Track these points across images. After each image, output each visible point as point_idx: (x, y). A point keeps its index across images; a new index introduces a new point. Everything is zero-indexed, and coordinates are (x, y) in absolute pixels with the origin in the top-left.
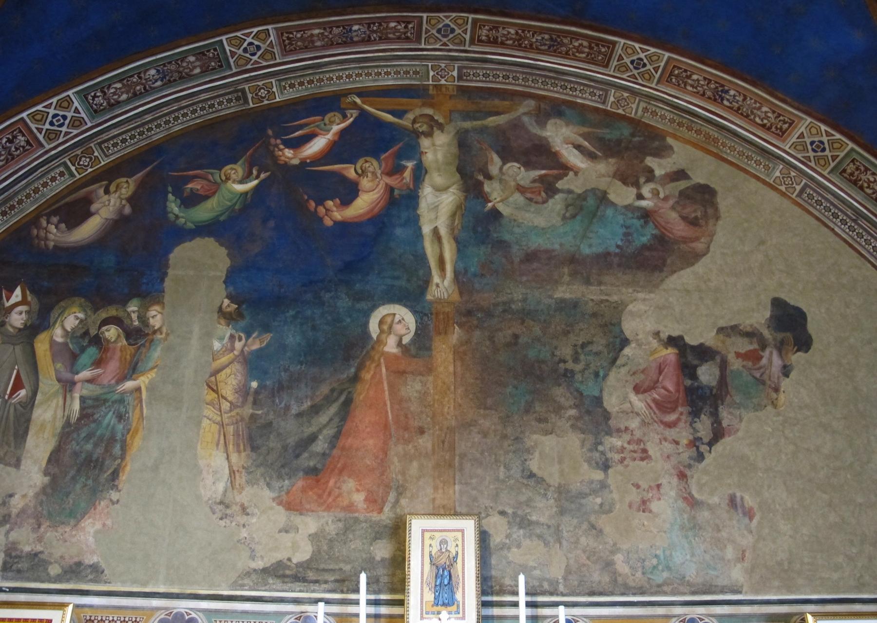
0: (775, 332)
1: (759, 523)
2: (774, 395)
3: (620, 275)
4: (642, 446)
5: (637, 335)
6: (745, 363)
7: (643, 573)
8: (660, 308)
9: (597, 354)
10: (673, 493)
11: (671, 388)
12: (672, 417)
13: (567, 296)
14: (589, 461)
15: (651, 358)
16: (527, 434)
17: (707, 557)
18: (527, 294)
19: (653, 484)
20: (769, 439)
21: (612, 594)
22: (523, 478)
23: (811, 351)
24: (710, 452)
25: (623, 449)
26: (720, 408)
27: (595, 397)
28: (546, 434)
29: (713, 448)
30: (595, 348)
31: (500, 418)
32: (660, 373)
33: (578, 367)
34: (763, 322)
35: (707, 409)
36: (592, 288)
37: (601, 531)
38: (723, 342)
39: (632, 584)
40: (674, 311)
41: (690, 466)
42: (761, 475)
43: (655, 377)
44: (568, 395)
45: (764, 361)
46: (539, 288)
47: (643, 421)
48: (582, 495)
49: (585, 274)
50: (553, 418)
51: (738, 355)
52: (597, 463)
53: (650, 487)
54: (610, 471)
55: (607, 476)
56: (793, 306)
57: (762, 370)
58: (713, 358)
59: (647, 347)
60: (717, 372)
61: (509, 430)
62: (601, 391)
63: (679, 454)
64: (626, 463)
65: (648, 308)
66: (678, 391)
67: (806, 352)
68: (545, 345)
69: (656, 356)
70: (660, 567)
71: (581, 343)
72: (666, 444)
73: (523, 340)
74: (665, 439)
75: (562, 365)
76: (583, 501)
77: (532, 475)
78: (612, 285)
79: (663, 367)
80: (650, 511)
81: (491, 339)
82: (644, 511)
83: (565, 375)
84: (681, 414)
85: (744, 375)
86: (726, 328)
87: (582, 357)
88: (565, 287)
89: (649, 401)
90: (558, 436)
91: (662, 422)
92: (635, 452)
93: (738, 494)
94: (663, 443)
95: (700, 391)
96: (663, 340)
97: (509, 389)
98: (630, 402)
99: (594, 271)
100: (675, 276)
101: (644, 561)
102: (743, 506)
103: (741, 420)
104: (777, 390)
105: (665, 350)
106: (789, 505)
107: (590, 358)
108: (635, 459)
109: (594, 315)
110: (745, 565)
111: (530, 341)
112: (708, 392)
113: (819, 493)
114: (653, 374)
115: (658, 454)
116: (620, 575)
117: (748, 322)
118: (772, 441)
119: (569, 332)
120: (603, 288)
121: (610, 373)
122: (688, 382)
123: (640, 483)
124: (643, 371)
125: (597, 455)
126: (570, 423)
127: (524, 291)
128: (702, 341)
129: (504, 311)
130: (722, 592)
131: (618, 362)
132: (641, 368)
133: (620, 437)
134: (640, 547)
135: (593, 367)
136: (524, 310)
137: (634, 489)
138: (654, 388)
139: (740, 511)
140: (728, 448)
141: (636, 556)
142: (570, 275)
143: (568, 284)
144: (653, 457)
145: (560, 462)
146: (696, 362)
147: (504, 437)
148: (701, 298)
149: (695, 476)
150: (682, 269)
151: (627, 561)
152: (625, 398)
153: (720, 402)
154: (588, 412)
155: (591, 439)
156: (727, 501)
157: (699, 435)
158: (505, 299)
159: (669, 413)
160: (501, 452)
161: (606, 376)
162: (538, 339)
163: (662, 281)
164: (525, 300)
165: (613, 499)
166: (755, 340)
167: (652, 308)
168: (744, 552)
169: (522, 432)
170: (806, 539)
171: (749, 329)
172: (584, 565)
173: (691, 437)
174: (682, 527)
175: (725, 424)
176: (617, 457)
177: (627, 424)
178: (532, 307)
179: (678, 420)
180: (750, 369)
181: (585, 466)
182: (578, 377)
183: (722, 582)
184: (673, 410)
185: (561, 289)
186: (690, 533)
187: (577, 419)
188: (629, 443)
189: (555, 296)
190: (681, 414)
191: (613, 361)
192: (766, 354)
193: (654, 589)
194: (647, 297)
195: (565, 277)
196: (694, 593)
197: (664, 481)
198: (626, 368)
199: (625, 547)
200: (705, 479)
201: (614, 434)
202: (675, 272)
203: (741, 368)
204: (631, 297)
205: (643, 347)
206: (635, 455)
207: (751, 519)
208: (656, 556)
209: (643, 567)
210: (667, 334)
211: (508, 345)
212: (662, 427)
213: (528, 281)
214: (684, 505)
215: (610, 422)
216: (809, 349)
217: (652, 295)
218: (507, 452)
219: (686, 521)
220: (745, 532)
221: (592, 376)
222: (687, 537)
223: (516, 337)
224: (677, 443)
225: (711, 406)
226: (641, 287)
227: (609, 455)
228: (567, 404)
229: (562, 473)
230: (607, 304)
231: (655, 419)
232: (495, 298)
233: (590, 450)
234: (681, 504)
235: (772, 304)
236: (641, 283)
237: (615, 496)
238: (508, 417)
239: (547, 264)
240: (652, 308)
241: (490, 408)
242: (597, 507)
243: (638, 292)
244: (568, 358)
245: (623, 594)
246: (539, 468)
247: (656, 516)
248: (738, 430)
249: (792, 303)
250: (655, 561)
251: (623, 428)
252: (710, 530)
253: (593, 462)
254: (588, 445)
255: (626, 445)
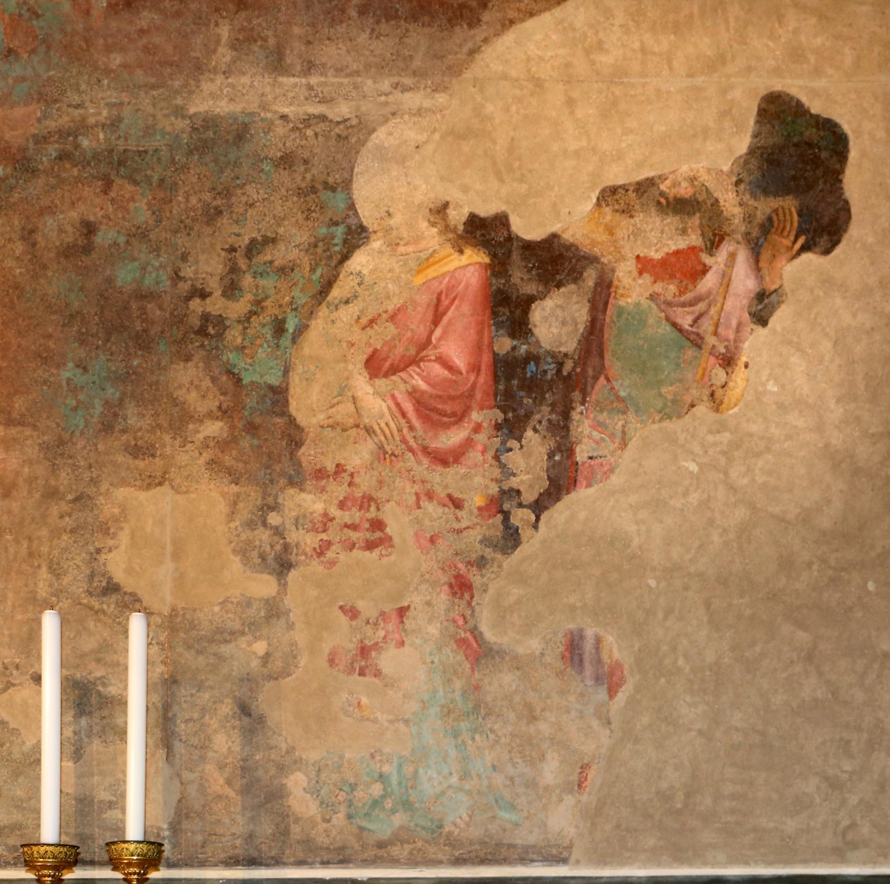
0: (754, 196)
1: (632, 702)
2: (720, 375)
3: (363, 37)
4: (372, 513)
5: (389, 214)
6: (658, 288)
7: (349, 817)
8: (459, 135)
9: (284, 271)
10: (433, 630)
11: (460, 362)
12: (452, 438)
13: (223, 107)
14: (243, 552)
15: (419, 280)
16: (104, 487)
17: (499, 780)
18: (121, 104)
19: (390, 607)
20: (685, 494)
21: (277, 862)
22: (90, 594)
23: (837, 251)
24: (536, 526)
25: (327, 519)
26: (575, 415)
27: (271, 388)
28: (149, 487)
29: (544, 517)
30: (280, 254)
31: (45, 447)
32: (436, 322)
33: (237, 308)
34: (726, 168)
35: (544, 413)
36: (287, 81)
37: (261, 719)
38: (610, 230)
39: (322, 840)
40: (494, 142)
41: (481, 563)
42: (652, 583)
43: (422, 331)
44: (207, 383)
45: (709, 281)
46: (153, 87)
47: (381, 447)
48: (224, 635)
49: (272, 41)
50: (167, 443)
51: (644, 265)
52: (263, 557)
53: (382, 614)
54: (293, 575)
55: (283, 585)
56: (817, 117)
57: (701, 307)
58: (576, 276)
59: (410, 249)
60: (581, 314)
61: (64, 478)
62: (286, 372)
63: (459, 531)
64: (330, 555)
65: (423, 137)
66: (475, 368)
67: (827, 252)
68: (156, 250)
69: (431, 273)
70: (389, 804)
71: (247, 241)
72: (430, 507)
73: (104, 237)
74: (430, 496)
75: (196, 304)
76: (226, 649)
77: (112, 588)
78: (339, 71)
79: (445, 302)
80: (378, 674)
81: (28, 235)
82: (362, 673)
83: (202, 332)
84: (477, 428)
85: (651, 321)
86: (625, 188)
87: (247, 281)
88: (219, 79)
89: (400, 397)
90: (177, 490)
91: (425, 450)
92: (354, 527)
93: (590, 633)
94: (425, 503)
95: (532, 367)
96: (454, 230)
97: (68, 372)
98: (354, 399)
99: (296, 30)
100: (509, 38)
101: (353, 787)
102: (599, 661)
103: (624, 445)
104: (728, 361)
105: (456, 255)
106: (710, 657)
107: (268, 283)
108: (352, 547)
109: (286, 161)
110: (585, 798)
111: (122, 239)
112: (551, 368)
113: (786, 629)
114: (417, 326)
115: (410, 533)
116: (297, 820)
117: (685, 168)
118: (694, 498)
119: (219, 212)
120: (314, 80)
121: (313, 323)
122: (504, 344)
123: (361, 605)
124: (392, 318)
125: (263, 536)
126: (207, 456)
127: (113, 96)
128: (556, 228)
129: (63, 156)
130: (523, 860)
131: (336, 293)
132: (391, 307)
133: (323, 490)
134: (347, 756)
135: (271, 310)
136: (111, 151)
137: (343, 619)
138: (415, 361)
139: (589, 670)
140: (582, 515)
141: (335, 777)
142: (235, 45)
143: (227, 74)
144: (396, 540)
145: (177, 556)
146: (530, 288)
147: (52, 494)
148: (570, 102)
149: (491, 591)
150: (532, 15)
151: (314, 791)
152: (343, 389)
153: (576, 395)
154: (252, 428)
155: (253, 495)
156: (562, 648)
157: (514, 482)
158: (64, 121)
159: (446, 426)
160: (44, 532)
161: (302, 329)
162: (141, 234)
163: (472, 53)
164: (114, 123)
165: (293, 644)
166: (696, 220)
167: (437, 136)
168: (584, 767)
169: (94, 481)
170: (737, 738)
171: (684, 190)
172: (220, 797)
173: (494, 489)
174: (447, 712)
175: (581, 454)
176: (310, 541)
177: (339, 459)
178: (132, 146)
179: (468, 443)
180: (669, 304)
181: (236, 563)
182: (234, 335)
183: (526, 837)
184: (459, 418)
185: (207, 87)
186: (464, 726)
187: (223, 445)
188: (342, 505)
189: (192, 110)
190: (477, 428)
191: (328, 285)
192: (717, 261)
193: (372, 853)
194: (427, 103)
195: (221, 50)
196: (458, 862)
197: (415, 600)
198: (353, 309)
199: (312, 756)
200: (516, 592)
201: (309, 484)
202: (512, 22)
203: (645, 303)
204: (386, 104)
205: (402, 249)
206: (354, 536)
207: (612, 692)
208: (382, 778)
209: (350, 804)
210: (465, 212)
211: (68, 252)
212: (426, 461)
213: (125, 66)
214: (461, 657)
215: (303, 450)
216: (835, 244)
217: (441, 98)
218: (56, 533)
219: (458, 695)
220: (595, 723)
221: (268, 332)
222: (456, 734)
223: (89, 228)
224: (457, 504)
225: (553, 405)
226: (414, 73)
227: (293, 536)
228: (202, 407)
229: (180, 580)
230: (321, 127)
231: (412, 442)
232: (39, 120)
233: (250, 525)
234: (452, 655)
235: (762, 113)
236: (417, 63)
237: (300, 636)
238: (61, 442)
239: (178, 14)
240: (437, 136)
241: (21, 423)
242: (255, 664)
243: (406, 89)
244: (214, 285)
245: (300, 863)
246: (129, 571)
247: (391, 684)
248: (612, 471)
249: (816, 107)
250: (377, 790)
251: (330, 467)
252: (512, 716)
253: (255, 554)
254: (245, 512)
255: (334, 511)
